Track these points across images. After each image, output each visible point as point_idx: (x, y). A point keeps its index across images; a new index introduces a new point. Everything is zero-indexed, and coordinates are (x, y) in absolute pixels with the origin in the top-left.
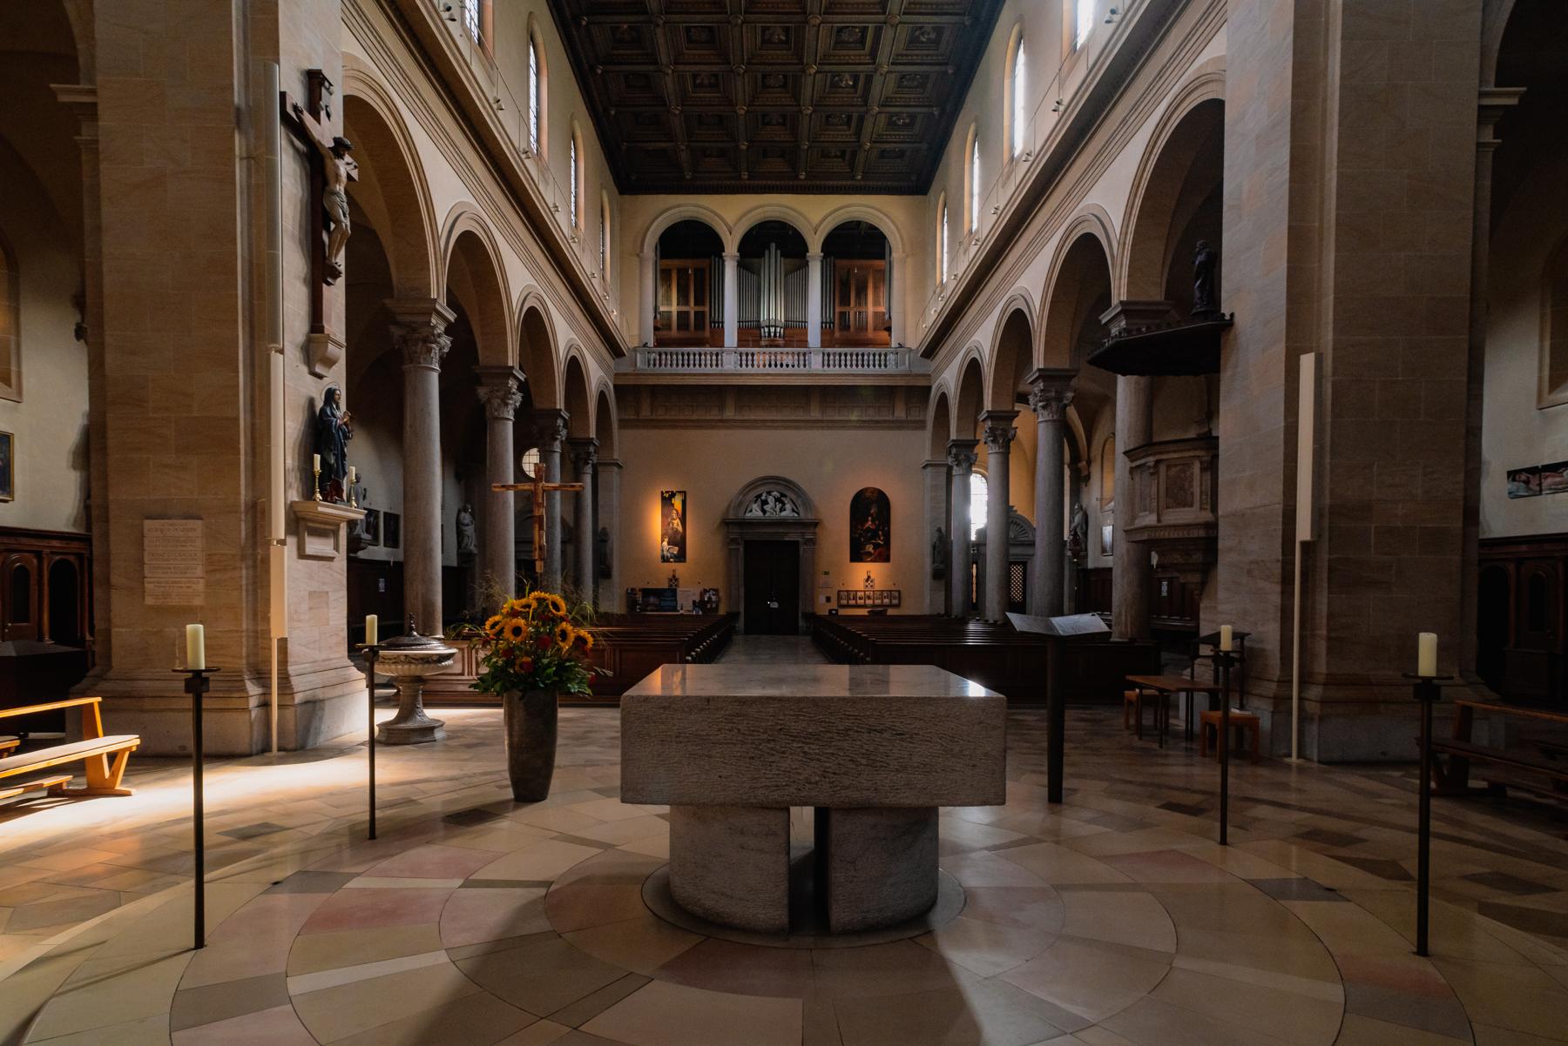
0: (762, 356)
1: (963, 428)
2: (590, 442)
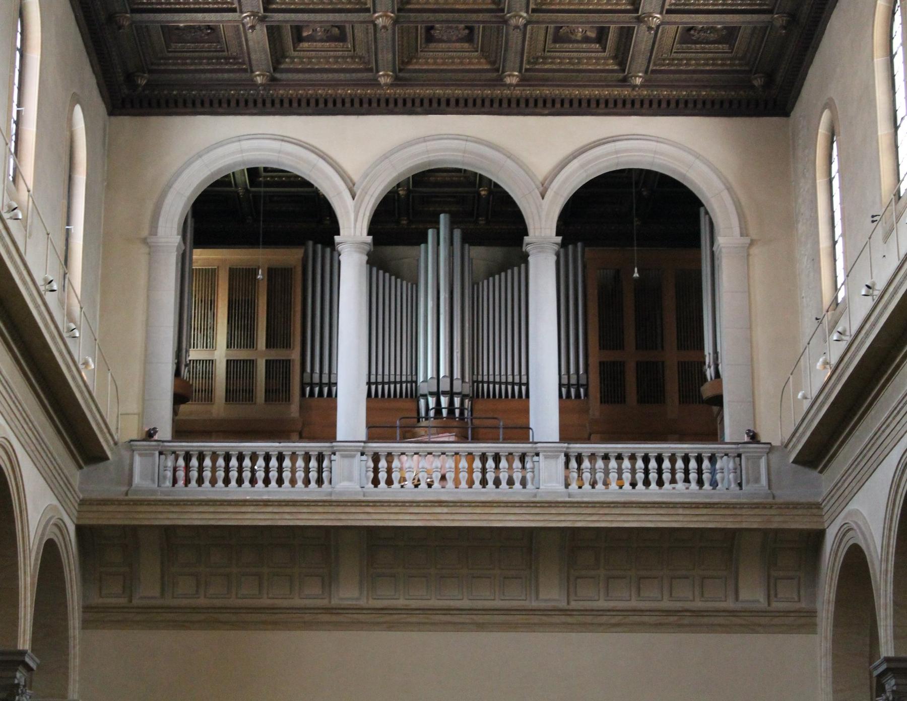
2: (16, 660)
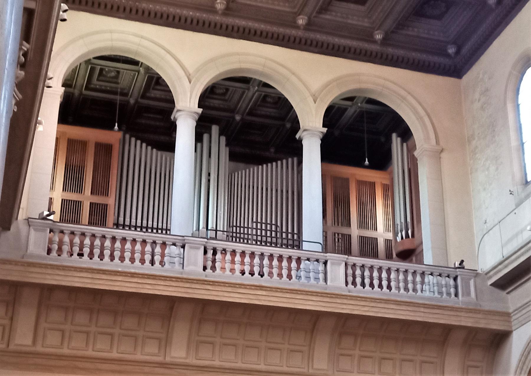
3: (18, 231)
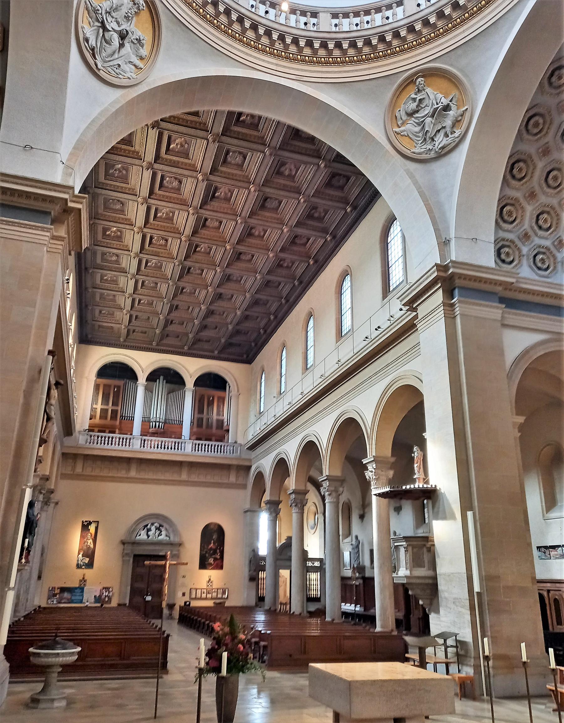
0: (156, 440)
1: (270, 491)
3: (76, 436)
